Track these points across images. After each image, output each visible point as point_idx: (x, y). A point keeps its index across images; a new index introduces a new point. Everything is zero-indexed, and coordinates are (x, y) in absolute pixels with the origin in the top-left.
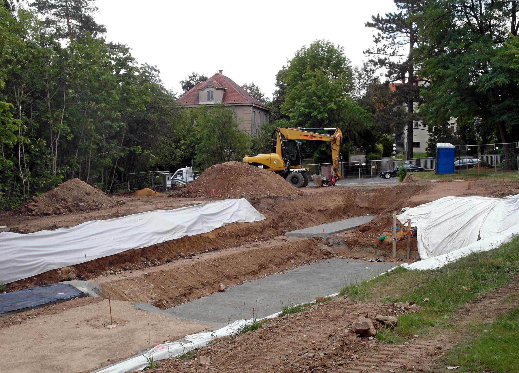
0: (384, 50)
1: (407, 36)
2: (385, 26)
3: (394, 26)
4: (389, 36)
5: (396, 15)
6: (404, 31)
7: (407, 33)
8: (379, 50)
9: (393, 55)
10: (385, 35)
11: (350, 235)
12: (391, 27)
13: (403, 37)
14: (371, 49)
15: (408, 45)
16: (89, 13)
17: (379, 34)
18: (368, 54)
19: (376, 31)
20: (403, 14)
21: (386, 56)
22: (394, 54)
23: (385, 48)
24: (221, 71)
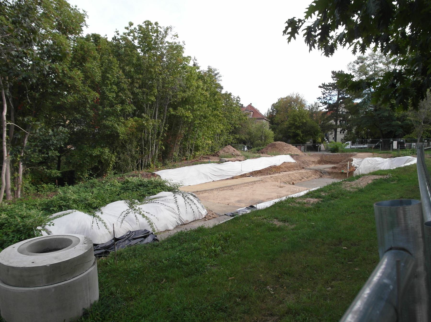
3: (331, 88)
5: (333, 84)
8: (324, 98)
11: (328, 170)
12: (330, 88)
13: (335, 92)
15: (337, 96)
16: (219, 82)
17: (324, 91)
18: (319, 99)
19: (323, 90)
21: (327, 100)
22: (330, 100)
24: (251, 104)
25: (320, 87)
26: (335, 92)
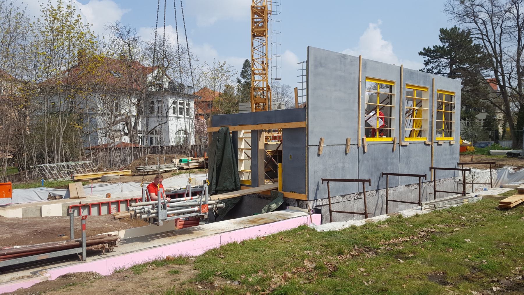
0: (432, 70)
1: (448, 61)
2: (433, 54)
4: (435, 60)
5: (440, 47)
6: (446, 57)
7: (448, 59)
8: (428, 70)
9: (438, 74)
10: (432, 61)
14: (423, 70)
19: (427, 58)
20: (445, 47)
23: (433, 69)
25: (421, 53)
26: (445, 60)
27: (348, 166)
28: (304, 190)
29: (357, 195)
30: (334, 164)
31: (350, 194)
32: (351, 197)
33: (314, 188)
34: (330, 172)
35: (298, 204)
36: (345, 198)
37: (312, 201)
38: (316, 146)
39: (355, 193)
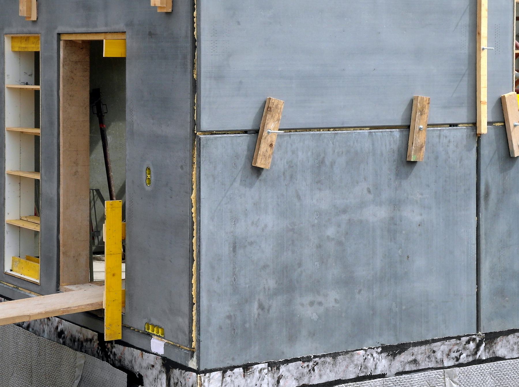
27: (418, 219)
28: (187, 321)
29: (472, 345)
30: (345, 211)
31: (434, 341)
32: (439, 355)
33: (229, 317)
34: (319, 246)
35: (168, 380)
36: (405, 357)
37: (217, 375)
38: (246, 132)
39: (459, 338)
